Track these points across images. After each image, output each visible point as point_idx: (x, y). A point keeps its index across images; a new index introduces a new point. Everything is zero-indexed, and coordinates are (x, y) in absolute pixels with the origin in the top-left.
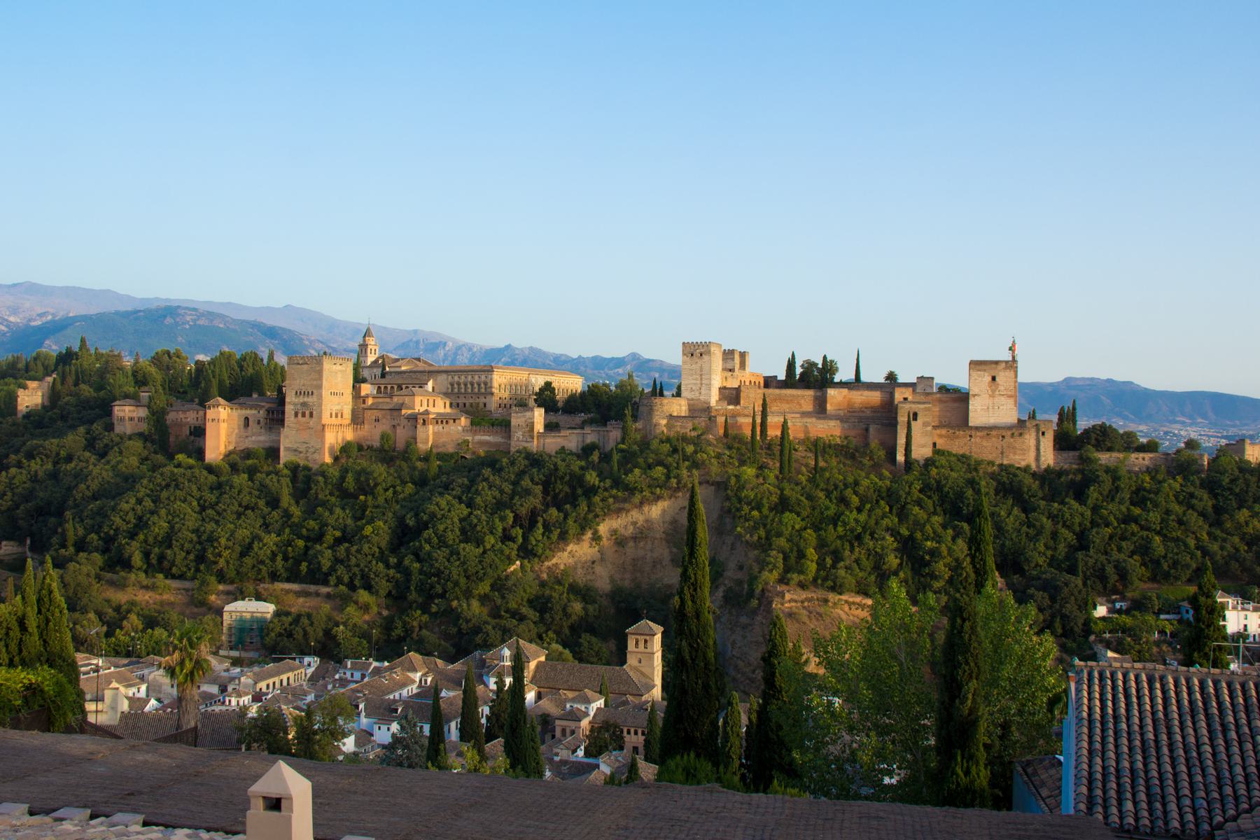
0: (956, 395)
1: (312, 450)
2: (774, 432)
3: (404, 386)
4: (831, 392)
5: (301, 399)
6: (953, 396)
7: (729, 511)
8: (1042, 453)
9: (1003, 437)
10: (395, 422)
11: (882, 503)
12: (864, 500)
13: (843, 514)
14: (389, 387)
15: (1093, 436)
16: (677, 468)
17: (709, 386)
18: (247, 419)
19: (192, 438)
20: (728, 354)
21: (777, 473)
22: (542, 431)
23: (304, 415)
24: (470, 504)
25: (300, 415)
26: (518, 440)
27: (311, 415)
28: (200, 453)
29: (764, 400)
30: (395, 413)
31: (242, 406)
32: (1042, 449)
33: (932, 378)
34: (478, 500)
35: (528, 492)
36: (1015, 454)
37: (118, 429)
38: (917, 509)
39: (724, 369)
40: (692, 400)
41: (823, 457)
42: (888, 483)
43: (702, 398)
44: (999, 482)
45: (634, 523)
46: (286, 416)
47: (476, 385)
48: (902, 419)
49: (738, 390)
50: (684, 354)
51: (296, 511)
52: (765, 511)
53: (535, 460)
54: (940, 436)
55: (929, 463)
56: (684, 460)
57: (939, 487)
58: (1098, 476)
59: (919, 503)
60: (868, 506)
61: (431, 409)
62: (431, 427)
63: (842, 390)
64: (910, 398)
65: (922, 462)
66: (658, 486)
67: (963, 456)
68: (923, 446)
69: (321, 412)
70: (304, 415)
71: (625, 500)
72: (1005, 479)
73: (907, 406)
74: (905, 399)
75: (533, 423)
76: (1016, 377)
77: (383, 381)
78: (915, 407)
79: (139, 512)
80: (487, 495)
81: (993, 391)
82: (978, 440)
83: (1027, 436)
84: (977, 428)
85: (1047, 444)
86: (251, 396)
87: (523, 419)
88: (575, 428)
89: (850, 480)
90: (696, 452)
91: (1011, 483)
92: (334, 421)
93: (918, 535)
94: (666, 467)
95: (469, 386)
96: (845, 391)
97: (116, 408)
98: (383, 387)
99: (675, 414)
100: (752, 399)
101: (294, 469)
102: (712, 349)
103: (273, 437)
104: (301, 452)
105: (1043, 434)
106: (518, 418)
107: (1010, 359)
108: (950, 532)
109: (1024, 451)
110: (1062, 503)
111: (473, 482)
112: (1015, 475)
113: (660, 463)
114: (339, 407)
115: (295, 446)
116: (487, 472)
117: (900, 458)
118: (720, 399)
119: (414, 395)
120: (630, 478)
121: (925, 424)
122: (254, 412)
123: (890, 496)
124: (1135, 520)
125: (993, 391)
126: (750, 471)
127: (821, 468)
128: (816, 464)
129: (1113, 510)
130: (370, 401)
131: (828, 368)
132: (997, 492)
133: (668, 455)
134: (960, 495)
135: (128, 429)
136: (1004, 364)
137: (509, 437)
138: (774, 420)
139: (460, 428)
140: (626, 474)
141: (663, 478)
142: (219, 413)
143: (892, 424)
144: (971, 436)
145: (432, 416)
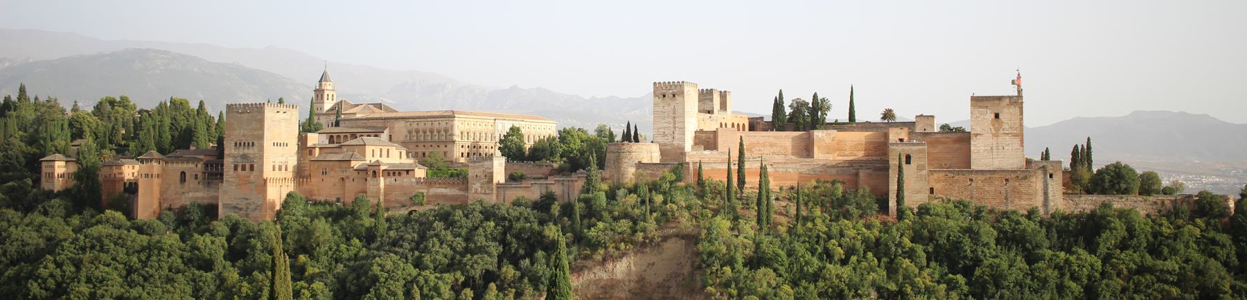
0: (958, 135)
1: (253, 206)
2: (752, 181)
3: (358, 135)
4: (818, 134)
5: (241, 151)
6: (954, 136)
7: (700, 267)
8: (1051, 198)
9: (1007, 180)
10: (344, 175)
11: (870, 255)
12: (850, 251)
13: (824, 268)
14: (342, 135)
15: (1107, 177)
16: (645, 221)
17: (683, 129)
18: (183, 174)
19: (127, 195)
20: (705, 95)
21: (754, 223)
22: (502, 181)
23: (244, 168)
24: (418, 264)
25: (239, 169)
26: (477, 193)
27: (252, 168)
28: (129, 213)
29: (741, 144)
30: (344, 165)
31: (179, 159)
32: (1050, 194)
33: (933, 117)
34: (427, 259)
35: (481, 250)
36: (1020, 198)
37: (45, 185)
38: (906, 262)
39: (700, 111)
40: (665, 145)
41: (806, 204)
42: (877, 233)
43: (675, 143)
44: (1000, 231)
45: (596, 282)
46: (225, 169)
47: (435, 133)
48: (893, 162)
49: (715, 133)
50: (655, 95)
51: (233, 275)
52: (739, 266)
53: (488, 214)
54: (938, 181)
55: (923, 211)
56: (651, 212)
57: (931, 239)
58: (1109, 222)
59: (911, 255)
60: (854, 258)
61: (384, 160)
62: (382, 179)
63: (829, 131)
64: (906, 139)
65: (916, 210)
66: (623, 240)
67: (960, 202)
68: (918, 192)
69: (262, 165)
70: (244, 168)
71: (586, 258)
72: (1007, 227)
73: (899, 148)
74: (901, 140)
75: (492, 173)
76: (1021, 113)
77: (336, 130)
78: (907, 149)
79: (60, 279)
80: (440, 252)
81: (997, 130)
82: (980, 184)
83: (1033, 179)
84: (977, 172)
85: (1056, 187)
86: (189, 148)
87: (482, 169)
88: (541, 178)
89: (835, 229)
90: (665, 202)
91: (1014, 230)
92: (277, 174)
93: (909, 290)
94: (635, 222)
95: (428, 133)
96: (834, 133)
97: (44, 164)
98: (335, 135)
99: (645, 161)
100: (728, 143)
101: (234, 228)
102: (686, 89)
103: (212, 193)
104: (241, 209)
105: (1051, 176)
106: (474, 168)
107: (1016, 94)
108: (943, 286)
109: (1031, 196)
110: (1069, 251)
111: (423, 237)
112: (1018, 223)
113: (626, 215)
114: (283, 159)
115: (234, 203)
116: (439, 225)
117: (892, 204)
118: (696, 144)
119: (365, 145)
120: (592, 233)
121: (920, 168)
122: (191, 165)
123: (877, 247)
124: (1151, 270)
125: (997, 130)
126: (723, 223)
127: (806, 219)
128: (797, 215)
129: (1128, 259)
130: (317, 151)
131: (818, 106)
132: (998, 241)
133: (633, 207)
134: (956, 246)
135: (58, 185)
136: (1008, 100)
137: (467, 189)
138: (751, 166)
139: (414, 180)
140: (589, 228)
141: (629, 231)
142: (153, 167)
143: (885, 168)
144: (971, 180)
145: (382, 168)
